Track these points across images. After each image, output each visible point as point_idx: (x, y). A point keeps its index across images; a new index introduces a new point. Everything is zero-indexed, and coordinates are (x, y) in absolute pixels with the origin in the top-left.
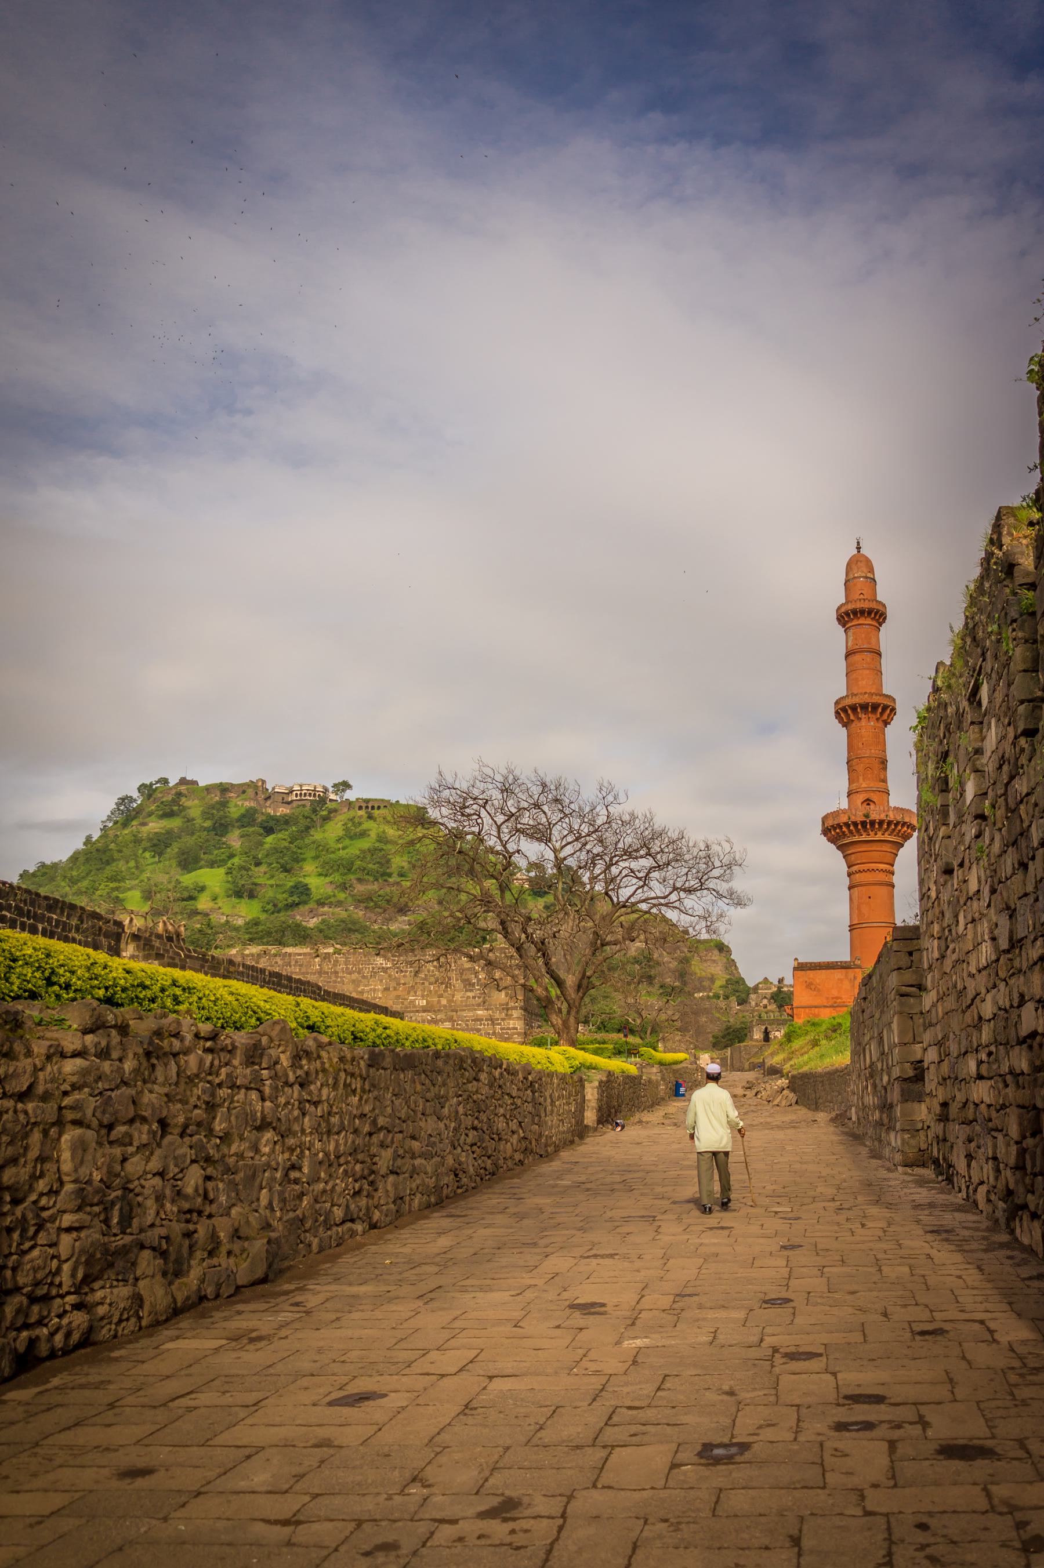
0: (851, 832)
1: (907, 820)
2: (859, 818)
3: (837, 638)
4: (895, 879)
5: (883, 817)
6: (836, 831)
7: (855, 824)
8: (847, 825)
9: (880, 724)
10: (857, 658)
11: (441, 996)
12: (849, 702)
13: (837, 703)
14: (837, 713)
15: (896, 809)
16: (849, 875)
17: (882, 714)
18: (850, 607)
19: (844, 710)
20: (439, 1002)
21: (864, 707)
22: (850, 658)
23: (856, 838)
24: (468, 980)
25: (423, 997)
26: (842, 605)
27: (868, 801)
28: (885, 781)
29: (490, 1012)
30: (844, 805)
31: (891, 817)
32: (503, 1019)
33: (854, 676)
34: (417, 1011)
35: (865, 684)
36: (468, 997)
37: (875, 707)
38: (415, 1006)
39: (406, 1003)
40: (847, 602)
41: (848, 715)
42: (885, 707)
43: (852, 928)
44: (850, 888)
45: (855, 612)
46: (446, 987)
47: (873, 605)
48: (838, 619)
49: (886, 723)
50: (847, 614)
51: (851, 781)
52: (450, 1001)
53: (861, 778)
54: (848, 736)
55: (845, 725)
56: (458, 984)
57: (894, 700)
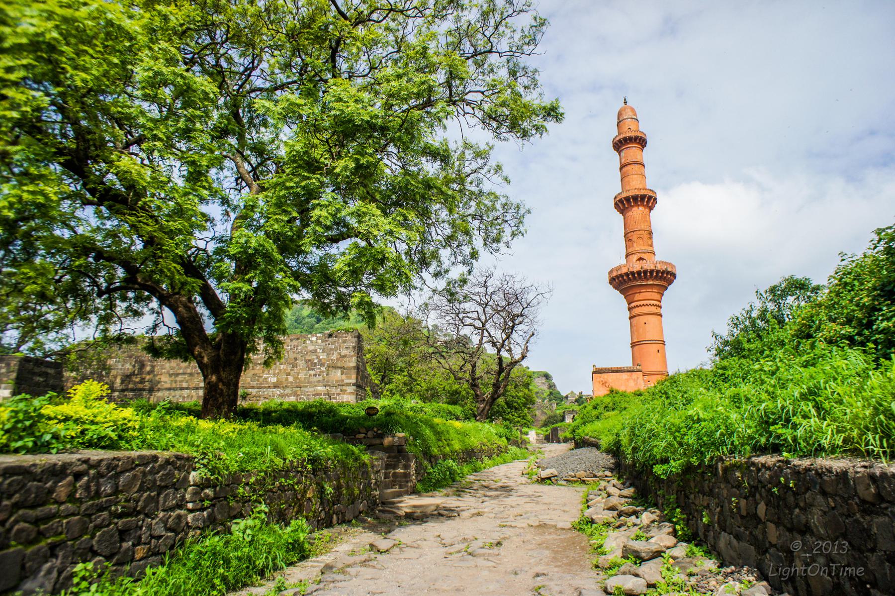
0: (630, 280)
1: (669, 269)
3: (614, 159)
4: (662, 311)
5: (652, 267)
7: (633, 273)
8: (627, 274)
9: (647, 210)
10: (629, 168)
12: (624, 195)
14: (616, 204)
15: (662, 262)
16: (629, 309)
17: (648, 202)
18: (622, 136)
19: (621, 201)
20: (287, 379)
21: (635, 198)
22: (625, 169)
23: (634, 283)
24: (310, 360)
28: (652, 246)
29: (328, 388)
32: (338, 394)
33: (626, 179)
34: (269, 387)
36: (310, 375)
37: (643, 197)
38: (267, 383)
39: (261, 380)
40: (619, 133)
41: (624, 205)
42: (650, 198)
43: (633, 345)
46: (293, 367)
48: (614, 146)
49: (651, 209)
50: (620, 141)
52: (296, 378)
53: (635, 245)
56: (301, 363)
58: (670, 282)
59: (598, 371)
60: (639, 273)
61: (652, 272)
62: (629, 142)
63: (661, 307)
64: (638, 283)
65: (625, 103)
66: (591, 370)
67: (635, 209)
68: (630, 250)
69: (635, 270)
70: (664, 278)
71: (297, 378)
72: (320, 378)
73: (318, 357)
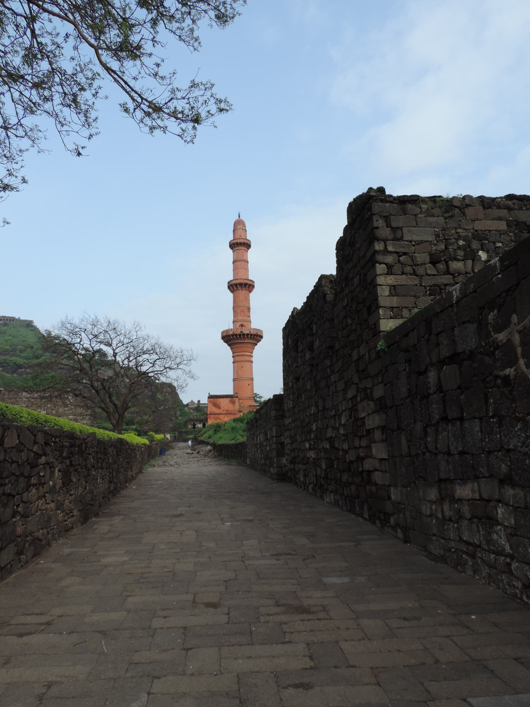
0: (234, 338)
2: (238, 332)
3: (229, 254)
4: (253, 359)
5: (248, 332)
6: (229, 338)
7: (236, 335)
8: (232, 335)
10: (238, 263)
11: (53, 409)
13: (229, 283)
15: (254, 329)
16: (233, 357)
18: (235, 241)
19: (232, 285)
23: (236, 341)
25: (44, 410)
26: (232, 240)
27: (242, 326)
28: (249, 317)
30: (231, 327)
31: (252, 332)
35: (241, 275)
36: (65, 410)
37: (246, 284)
40: (234, 240)
41: (234, 288)
42: (250, 285)
43: (234, 380)
44: (233, 363)
45: (237, 244)
47: (246, 241)
49: (250, 292)
50: (234, 244)
51: (235, 316)
52: (57, 412)
53: (239, 315)
54: (234, 297)
55: (232, 292)
57: (254, 282)
58: (259, 341)
59: (211, 397)
60: (240, 335)
61: (248, 335)
62: (240, 245)
63: (252, 357)
64: (239, 341)
65: (239, 216)
66: (208, 395)
67: (240, 291)
68: (236, 319)
69: (238, 333)
70: (257, 337)
71: (58, 412)
72: (71, 412)
73: (70, 401)
